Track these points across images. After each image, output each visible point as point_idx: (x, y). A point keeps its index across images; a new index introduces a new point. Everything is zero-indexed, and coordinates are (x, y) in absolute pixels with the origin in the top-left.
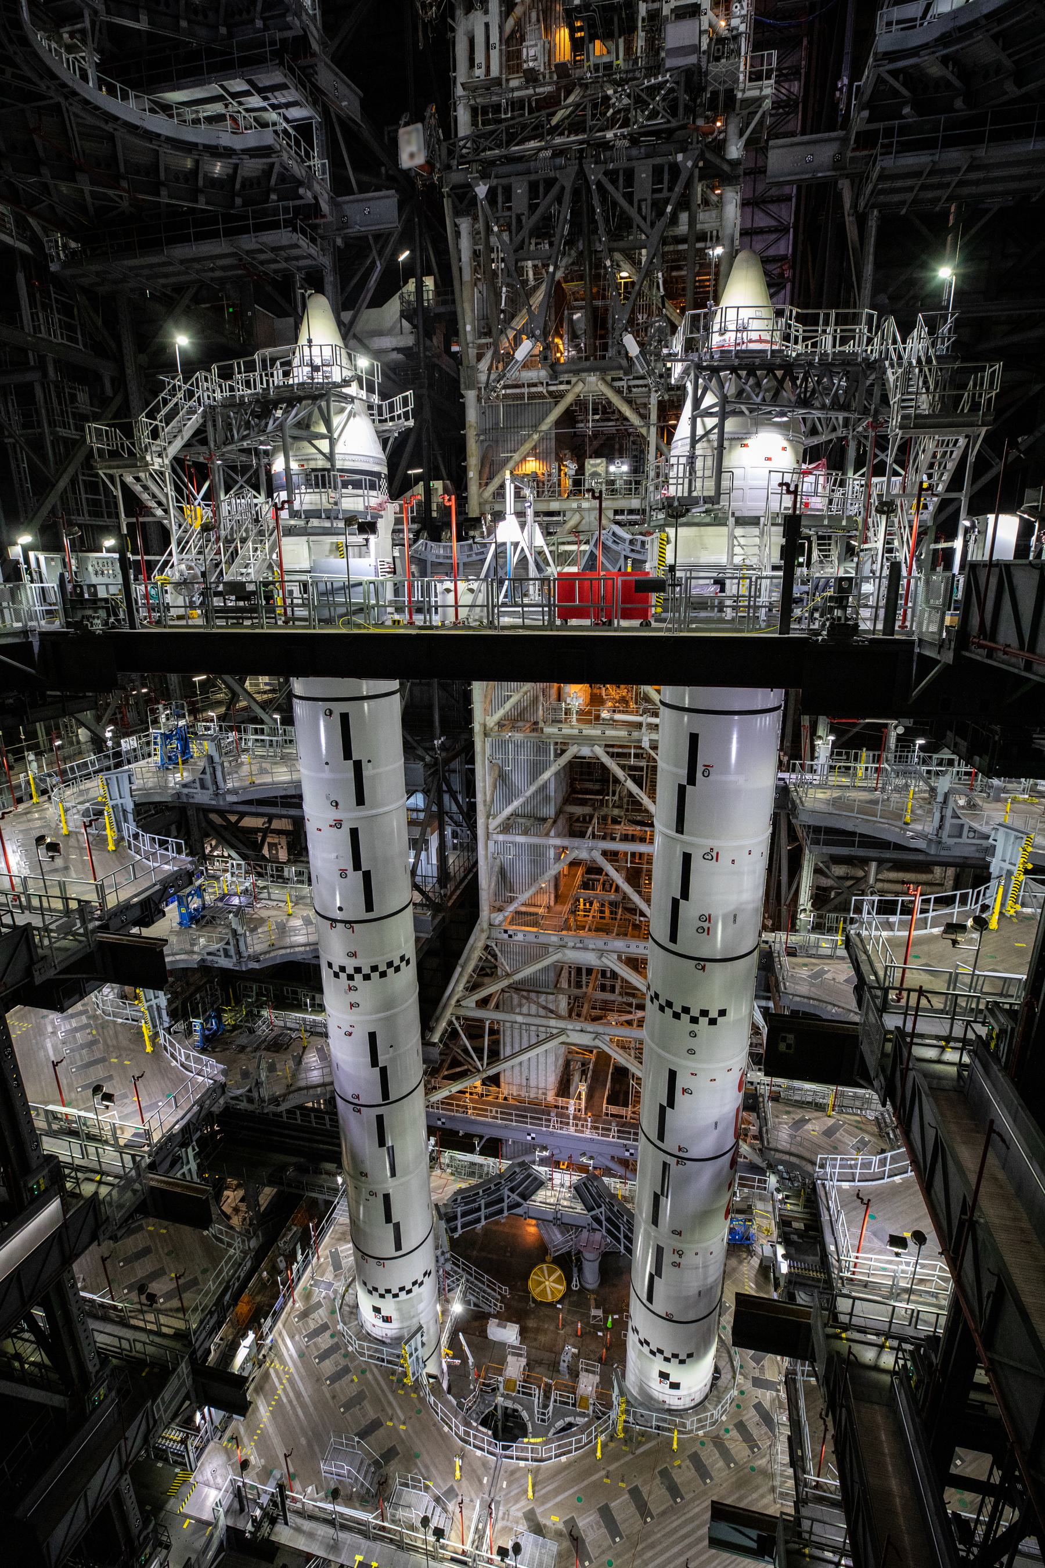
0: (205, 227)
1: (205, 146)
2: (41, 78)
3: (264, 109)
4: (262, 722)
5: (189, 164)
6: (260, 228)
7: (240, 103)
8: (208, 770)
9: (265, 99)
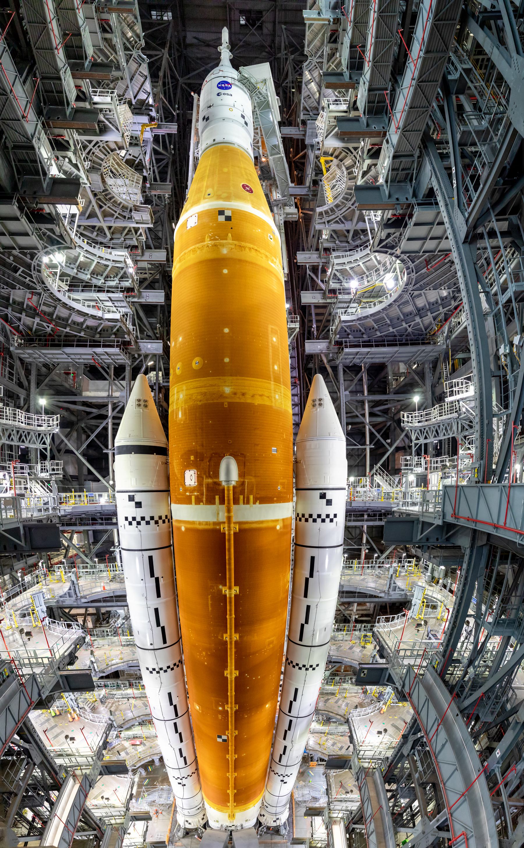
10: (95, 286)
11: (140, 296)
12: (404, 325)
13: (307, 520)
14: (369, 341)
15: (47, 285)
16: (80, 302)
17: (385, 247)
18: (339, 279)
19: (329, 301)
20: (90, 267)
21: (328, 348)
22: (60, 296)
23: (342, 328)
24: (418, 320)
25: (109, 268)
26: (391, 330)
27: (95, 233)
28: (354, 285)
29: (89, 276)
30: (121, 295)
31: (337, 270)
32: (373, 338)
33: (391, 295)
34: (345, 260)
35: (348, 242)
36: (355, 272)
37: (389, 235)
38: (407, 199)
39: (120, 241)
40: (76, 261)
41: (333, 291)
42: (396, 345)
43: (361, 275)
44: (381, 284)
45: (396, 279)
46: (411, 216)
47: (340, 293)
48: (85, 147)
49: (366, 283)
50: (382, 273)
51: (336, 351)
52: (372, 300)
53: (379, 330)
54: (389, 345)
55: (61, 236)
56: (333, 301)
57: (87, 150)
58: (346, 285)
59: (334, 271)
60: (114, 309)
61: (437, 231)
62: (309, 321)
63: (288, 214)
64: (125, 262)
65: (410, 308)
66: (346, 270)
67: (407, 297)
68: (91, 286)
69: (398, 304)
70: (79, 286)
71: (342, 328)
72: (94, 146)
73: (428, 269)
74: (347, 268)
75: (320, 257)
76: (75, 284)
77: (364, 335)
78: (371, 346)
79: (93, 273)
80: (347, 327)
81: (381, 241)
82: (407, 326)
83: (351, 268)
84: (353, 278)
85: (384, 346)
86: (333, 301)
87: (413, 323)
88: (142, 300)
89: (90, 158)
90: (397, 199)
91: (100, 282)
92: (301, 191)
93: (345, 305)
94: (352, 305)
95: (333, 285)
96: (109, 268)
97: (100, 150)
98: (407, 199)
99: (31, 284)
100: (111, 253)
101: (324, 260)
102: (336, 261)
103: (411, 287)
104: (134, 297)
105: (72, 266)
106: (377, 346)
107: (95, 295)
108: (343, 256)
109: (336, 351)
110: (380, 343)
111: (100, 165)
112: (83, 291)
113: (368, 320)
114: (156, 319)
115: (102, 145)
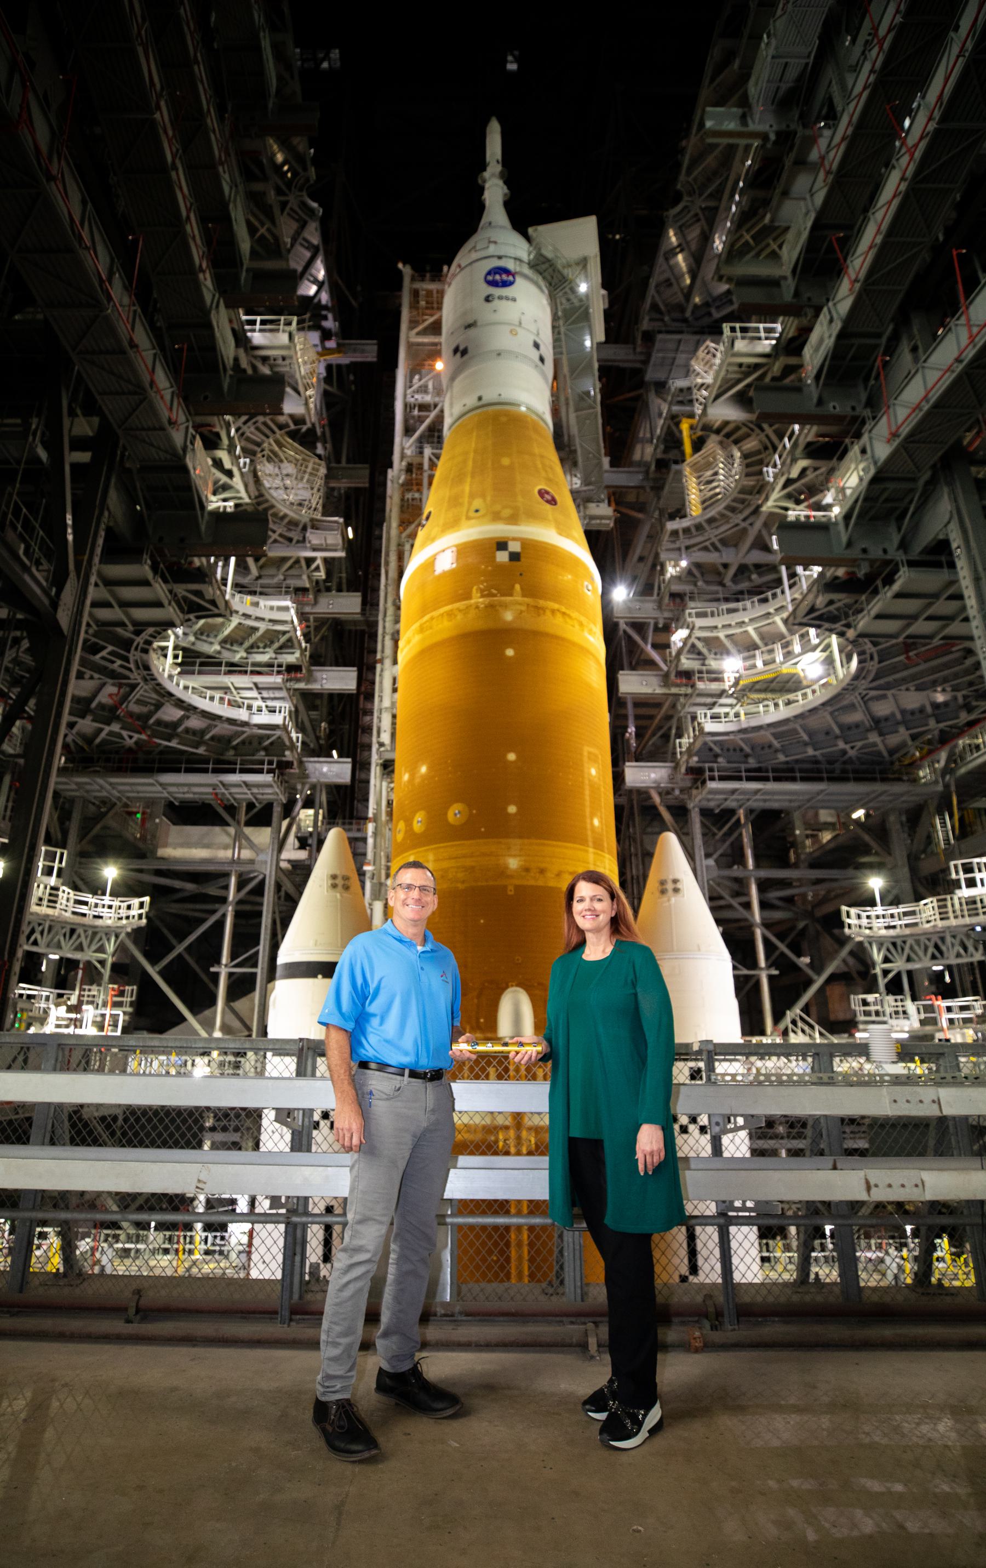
6: (243, 771)
11: (310, 678)
12: (841, 745)
14: (759, 770)
17: (820, 618)
18: (699, 653)
19: (674, 690)
21: (671, 779)
23: (705, 744)
24: (874, 738)
26: (810, 752)
28: (732, 667)
30: (278, 679)
31: (699, 639)
32: (770, 764)
33: (814, 692)
34: (718, 621)
35: (722, 584)
36: (735, 643)
37: (831, 602)
38: (885, 551)
41: (687, 675)
42: (820, 779)
43: (749, 648)
44: (792, 671)
45: (829, 661)
46: (889, 581)
47: (700, 679)
49: (759, 663)
50: (797, 648)
51: (689, 784)
52: (769, 696)
53: (783, 750)
54: (803, 779)
55: (213, 602)
56: (683, 690)
58: (713, 664)
59: (693, 640)
61: (943, 607)
62: (641, 728)
63: (592, 518)
65: (857, 716)
66: (717, 638)
67: (854, 698)
68: (220, 664)
69: (829, 709)
70: (193, 664)
71: (705, 744)
73: (908, 658)
74: (721, 635)
75: (660, 607)
77: (747, 756)
78: (766, 779)
79: (224, 642)
80: (715, 743)
82: (847, 747)
83: (727, 636)
84: (728, 653)
85: (793, 779)
86: (683, 690)
87: (859, 744)
88: (315, 686)
90: (864, 551)
91: (239, 655)
92: (621, 478)
93: (709, 700)
94: (723, 701)
95: (687, 663)
98: (885, 551)
101: (667, 615)
102: (700, 622)
103: (863, 684)
104: (298, 680)
106: (776, 779)
107: (228, 680)
108: (713, 615)
109: (689, 784)
110: (784, 774)
112: (200, 673)
113: (762, 732)
114: (342, 724)
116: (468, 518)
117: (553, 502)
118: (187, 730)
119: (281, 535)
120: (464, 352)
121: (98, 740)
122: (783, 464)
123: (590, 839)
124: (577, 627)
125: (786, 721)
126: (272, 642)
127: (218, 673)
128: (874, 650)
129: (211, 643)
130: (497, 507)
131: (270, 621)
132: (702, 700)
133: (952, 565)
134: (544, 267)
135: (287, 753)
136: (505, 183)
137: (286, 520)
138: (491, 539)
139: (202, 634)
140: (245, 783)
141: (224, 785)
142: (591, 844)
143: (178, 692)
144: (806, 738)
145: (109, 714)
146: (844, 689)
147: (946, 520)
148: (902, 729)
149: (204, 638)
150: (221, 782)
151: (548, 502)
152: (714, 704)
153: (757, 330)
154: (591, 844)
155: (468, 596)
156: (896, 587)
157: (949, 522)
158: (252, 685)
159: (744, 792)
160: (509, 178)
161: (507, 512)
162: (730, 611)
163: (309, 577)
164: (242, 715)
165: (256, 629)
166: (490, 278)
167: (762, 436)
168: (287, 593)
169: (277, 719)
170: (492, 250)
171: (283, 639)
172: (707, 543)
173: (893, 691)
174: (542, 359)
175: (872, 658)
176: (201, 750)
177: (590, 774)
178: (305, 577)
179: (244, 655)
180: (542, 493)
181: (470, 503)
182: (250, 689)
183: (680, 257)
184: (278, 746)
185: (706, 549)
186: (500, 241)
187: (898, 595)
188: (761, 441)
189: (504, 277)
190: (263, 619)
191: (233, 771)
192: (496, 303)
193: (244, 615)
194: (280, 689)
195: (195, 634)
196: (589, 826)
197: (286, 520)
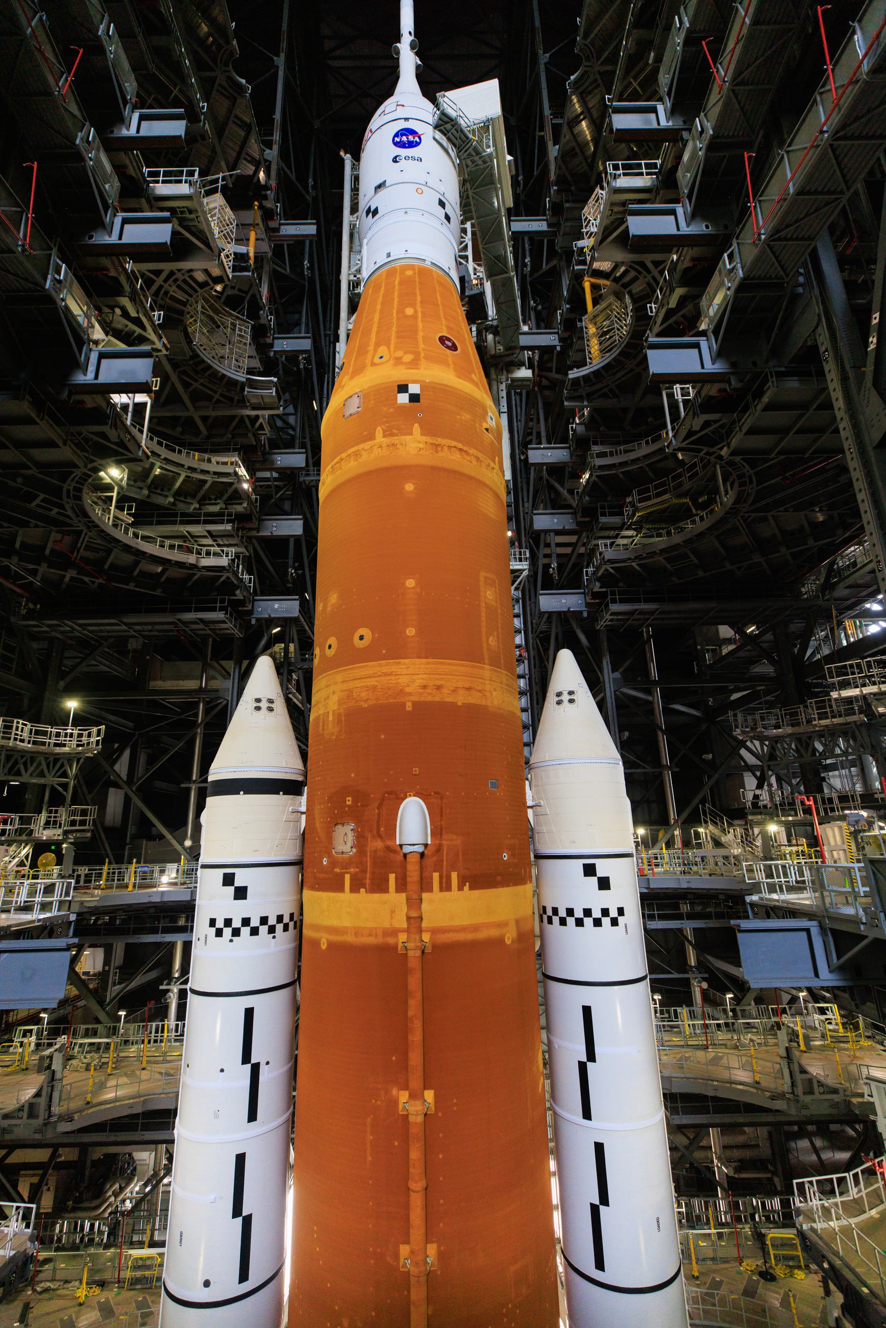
0: (153, 606)
1: (177, 562)
2: (77, 516)
3: (212, 546)
4: (98, 1021)
5: (160, 569)
7: (196, 541)
8: (44, 1093)
9: (214, 541)
10: (183, 515)
13: (563, 922)
15: (94, 518)
16: (156, 545)
20: (173, 484)
22: (119, 534)
25: (207, 486)
27: (179, 429)
29: (171, 500)
30: (229, 527)
37: (707, 424)
39: (225, 439)
40: (147, 476)
48: (148, 283)
57: (154, 288)
60: (217, 549)
64: (236, 473)
68: (176, 515)
72: (165, 281)
76: (146, 514)
79: (178, 494)
81: (690, 433)
89: (160, 301)
96: (207, 486)
97: (179, 287)
99: (62, 518)
100: (209, 461)
105: (139, 484)
111: (182, 313)
112: (159, 523)
115: (181, 278)
116: (373, 364)
117: (454, 348)
118: (143, 574)
119: (221, 395)
120: (376, 212)
121: (64, 586)
122: (664, 296)
123: (486, 657)
124: (474, 462)
125: (676, 547)
126: (222, 494)
127: (174, 523)
128: (752, 472)
129: (166, 496)
130: (399, 354)
131: (215, 473)
132: (607, 533)
133: (821, 374)
134: (448, 126)
135: (238, 592)
136: (417, 54)
137: (225, 381)
138: (396, 382)
139: (156, 488)
140: (200, 619)
141: (183, 623)
142: (487, 661)
143: (127, 538)
144: (696, 561)
145: (61, 560)
146: (726, 513)
147: (814, 325)
148: (783, 550)
149: (158, 491)
150: (179, 620)
151: (448, 347)
152: (616, 537)
153: (639, 166)
154: (487, 661)
155: (372, 437)
156: (765, 399)
157: (817, 327)
158: (206, 534)
159: (642, 612)
160: (421, 48)
161: (408, 358)
162: (626, 451)
163: (255, 435)
164: (191, 559)
165: (205, 481)
166: (397, 139)
167: (649, 278)
168: (235, 450)
169: (224, 561)
170: (401, 113)
171: (230, 491)
172: (606, 390)
173: (772, 513)
174: (448, 218)
175: (751, 482)
176: (158, 592)
177: (485, 597)
178: (250, 435)
179: (197, 506)
180: (442, 340)
181: (375, 350)
182: (205, 537)
183: (584, 123)
184: (229, 587)
185: (605, 396)
186: (407, 103)
187: (768, 408)
188: (649, 284)
189: (411, 138)
190: (208, 472)
191: (189, 610)
192: (403, 163)
193: (189, 468)
194: (231, 536)
195: (149, 488)
196: (485, 645)
197: (225, 381)
